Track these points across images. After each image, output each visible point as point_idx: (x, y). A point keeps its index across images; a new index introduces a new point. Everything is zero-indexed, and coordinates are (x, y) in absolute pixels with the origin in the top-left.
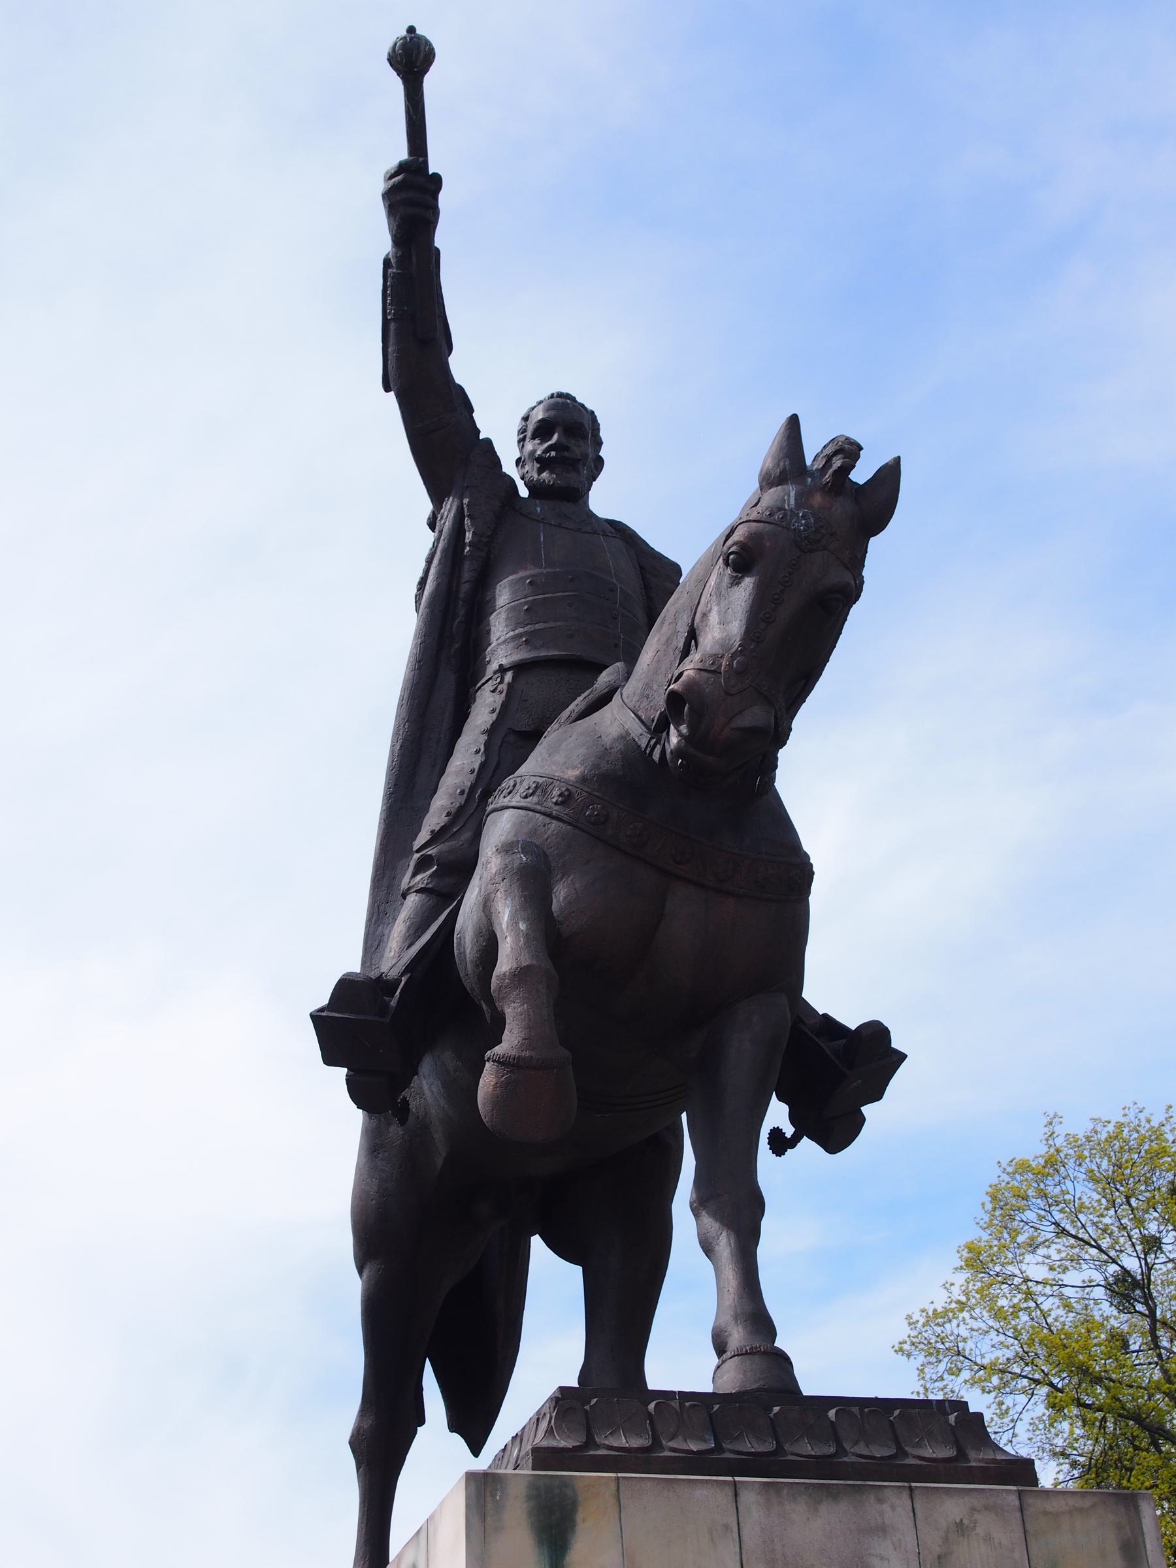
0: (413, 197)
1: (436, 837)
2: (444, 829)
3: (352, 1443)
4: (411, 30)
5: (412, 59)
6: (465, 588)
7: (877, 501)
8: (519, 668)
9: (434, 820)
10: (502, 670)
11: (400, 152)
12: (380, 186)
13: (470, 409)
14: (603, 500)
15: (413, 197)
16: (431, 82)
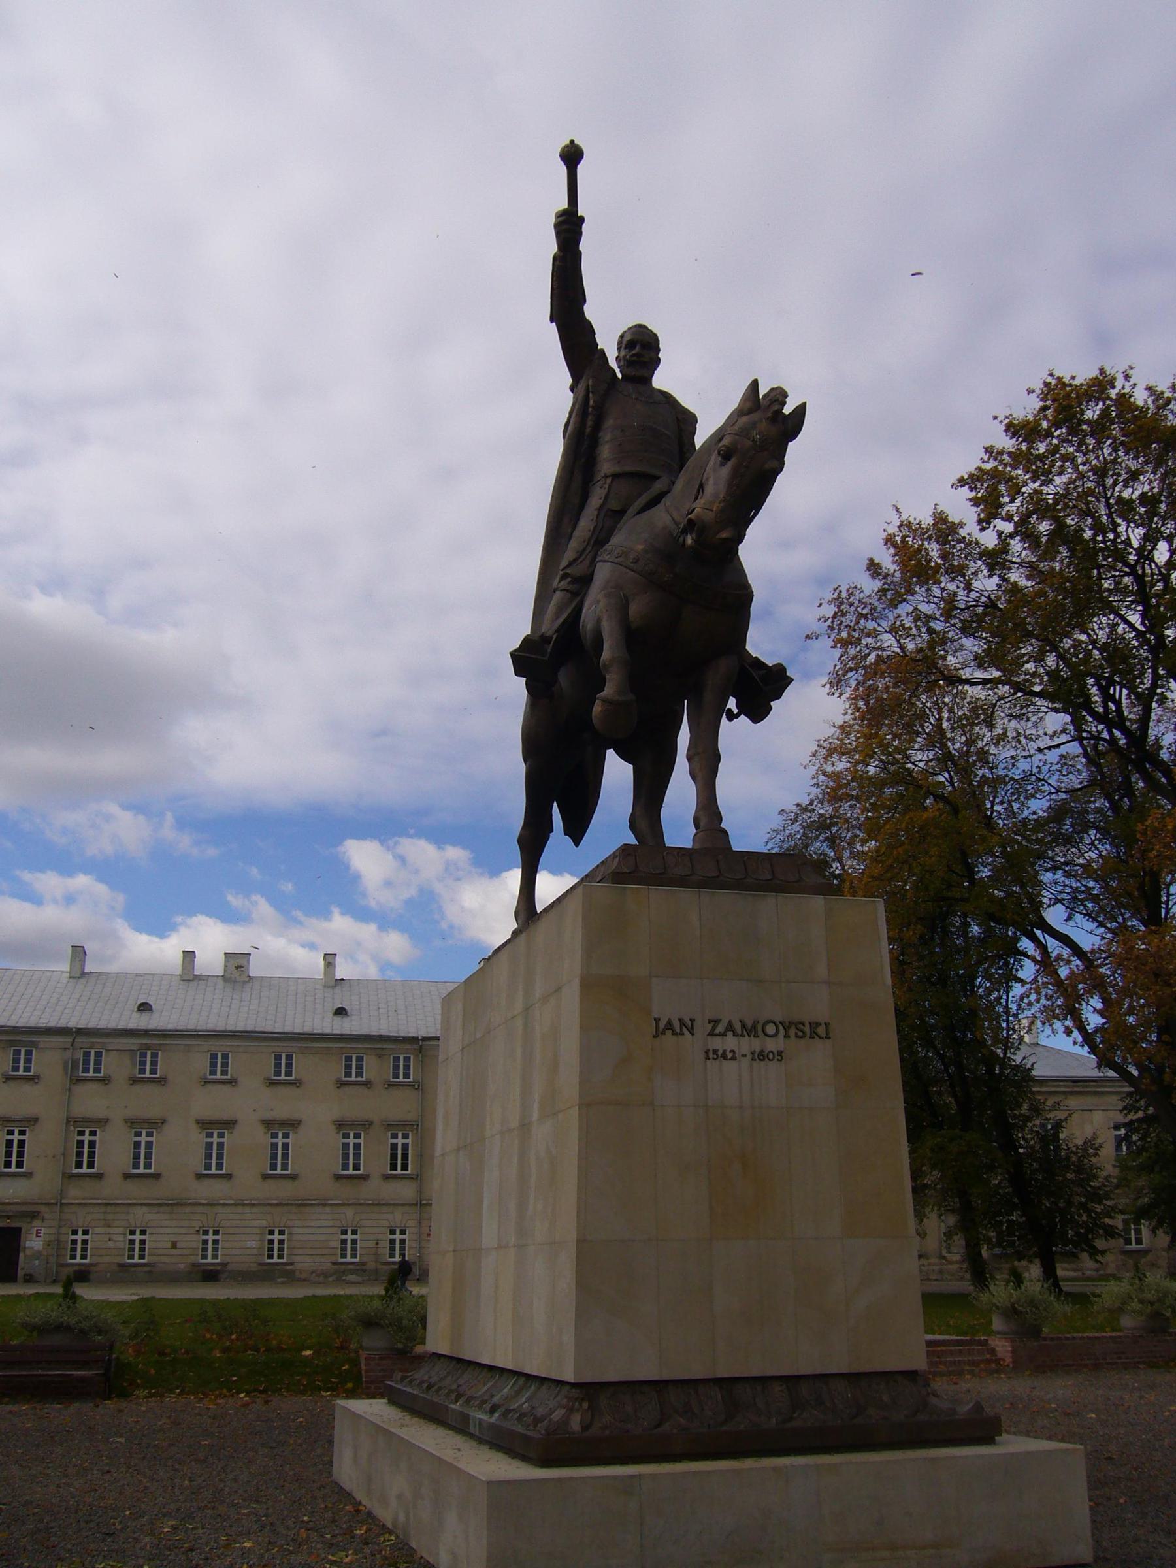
0: (569, 226)
1: (570, 564)
2: (575, 560)
3: (518, 841)
4: (572, 142)
5: (572, 156)
6: (588, 430)
7: (794, 424)
8: (615, 476)
9: (569, 555)
10: (606, 477)
11: (564, 204)
12: (552, 220)
13: (593, 332)
14: (660, 381)
15: (569, 226)
16: (581, 168)
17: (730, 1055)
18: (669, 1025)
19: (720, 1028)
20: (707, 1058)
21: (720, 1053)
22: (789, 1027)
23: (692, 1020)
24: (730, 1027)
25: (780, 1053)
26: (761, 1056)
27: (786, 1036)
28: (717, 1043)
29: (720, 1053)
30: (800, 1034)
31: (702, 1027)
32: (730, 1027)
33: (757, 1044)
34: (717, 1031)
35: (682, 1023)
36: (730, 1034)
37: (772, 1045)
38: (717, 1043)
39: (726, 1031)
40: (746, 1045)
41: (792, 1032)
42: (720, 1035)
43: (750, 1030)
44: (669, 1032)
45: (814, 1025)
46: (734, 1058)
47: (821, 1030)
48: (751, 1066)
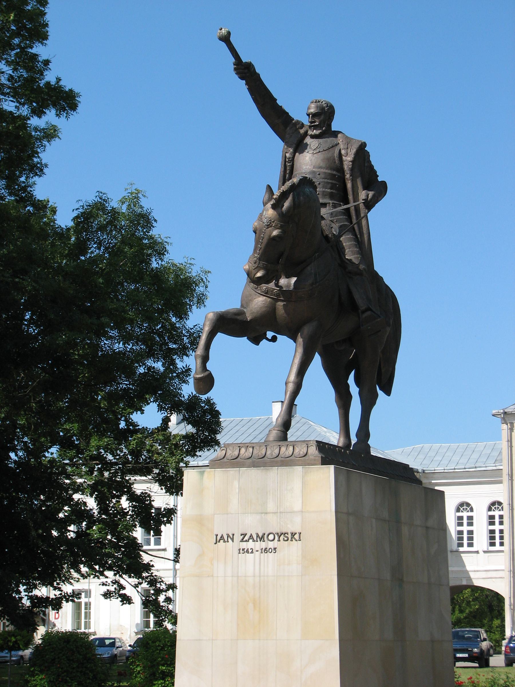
17: (250, 551)
18: (222, 537)
19: (246, 538)
20: (240, 553)
21: (245, 550)
22: (281, 535)
23: (241, 535)
24: (251, 537)
25: (275, 549)
26: (266, 550)
27: (279, 540)
28: (244, 545)
29: (245, 550)
30: (286, 539)
31: (238, 538)
32: (251, 537)
33: (263, 545)
34: (244, 540)
35: (228, 536)
36: (251, 540)
37: (271, 545)
38: (244, 545)
39: (249, 539)
40: (259, 545)
41: (282, 537)
42: (246, 541)
43: (262, 538)
44: (222, 541)
45: (293, 534)
46: (252, 552)
47: (296, 536)
48: (260, 555)
